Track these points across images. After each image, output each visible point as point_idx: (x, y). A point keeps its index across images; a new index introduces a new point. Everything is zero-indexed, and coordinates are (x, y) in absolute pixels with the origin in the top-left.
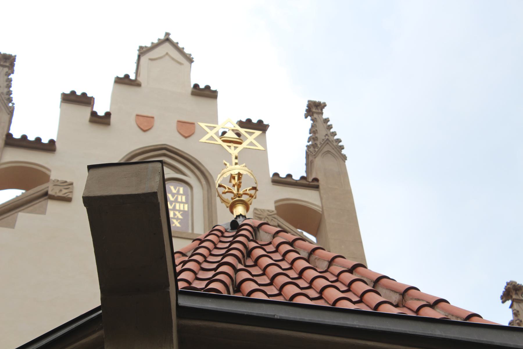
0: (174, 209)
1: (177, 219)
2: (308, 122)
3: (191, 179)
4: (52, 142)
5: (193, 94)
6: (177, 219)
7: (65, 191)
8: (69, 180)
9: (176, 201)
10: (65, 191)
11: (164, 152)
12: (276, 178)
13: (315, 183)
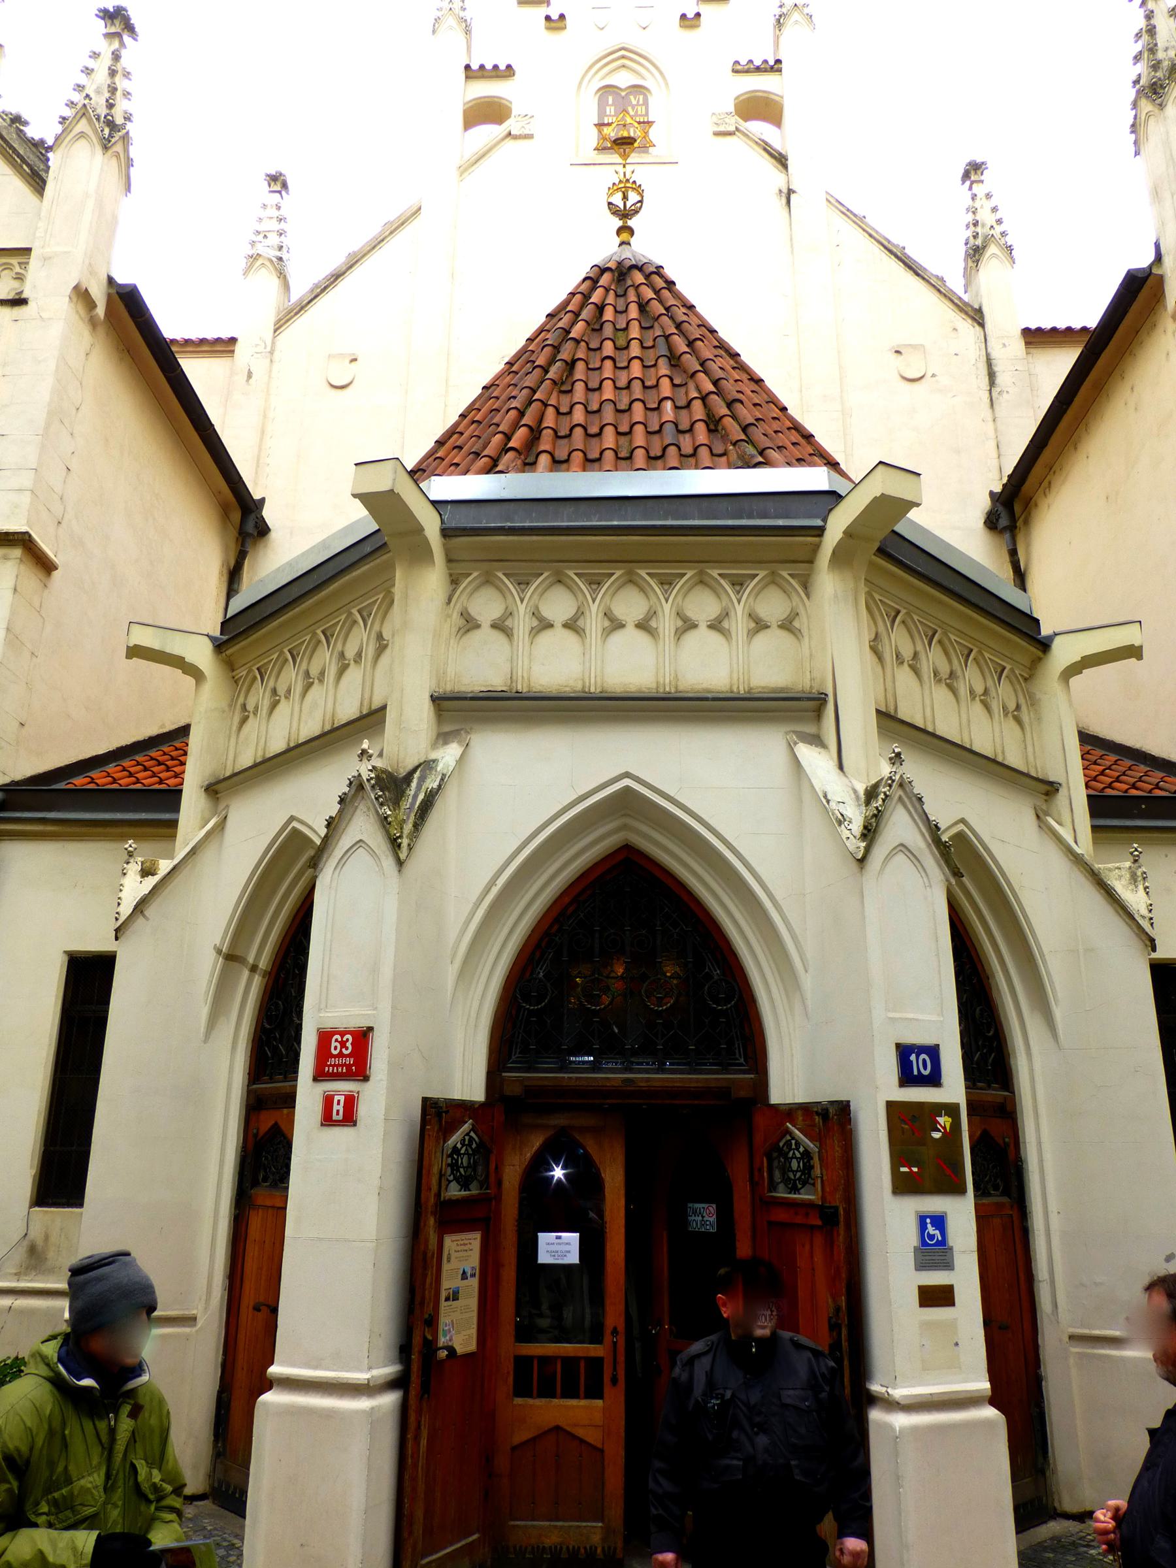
4: (509, 67)
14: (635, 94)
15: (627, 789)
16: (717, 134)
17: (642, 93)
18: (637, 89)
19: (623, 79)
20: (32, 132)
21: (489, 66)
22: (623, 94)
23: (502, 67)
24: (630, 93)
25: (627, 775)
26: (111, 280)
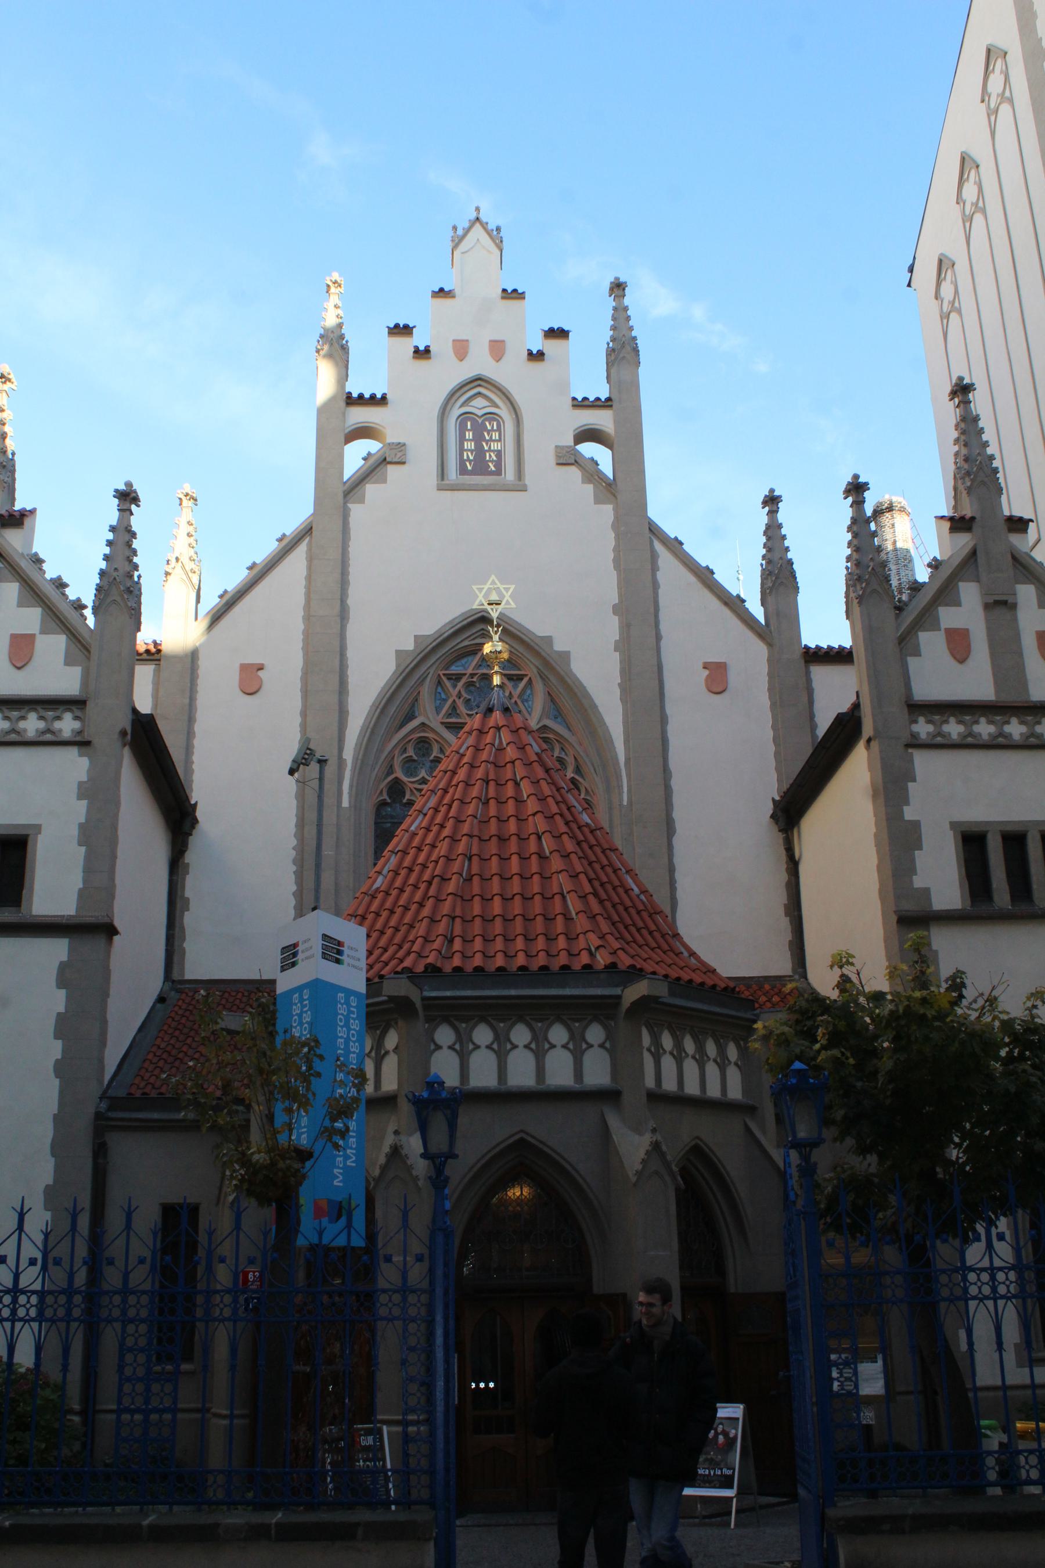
0: (490, 450)
1: (492, 461)
2: (611, 303)
3: (504, 412)
5: (503, 298)
6: (492, 461)
7: (399, 454)
8: (402, 441)
9: (491, 440)
10: (399, 454)
11: (479, 382)
12: (576, 403)
13: (609, 403)
14: (490, 420)
15: (522, 1140)
16: (558, 464)
17: (495, 420)
18: (491, 416)
19: (479, 406)
20: (72, 594)
21: (367, 396)
22: (480, 421)
23: (379, 396)
24: (486, 419)
25: (522, 1131)
26: (135, 711)
